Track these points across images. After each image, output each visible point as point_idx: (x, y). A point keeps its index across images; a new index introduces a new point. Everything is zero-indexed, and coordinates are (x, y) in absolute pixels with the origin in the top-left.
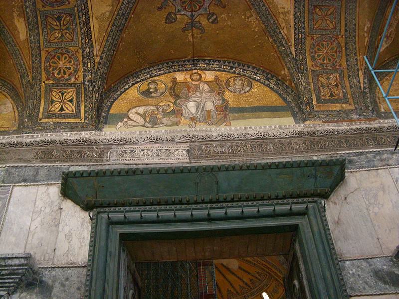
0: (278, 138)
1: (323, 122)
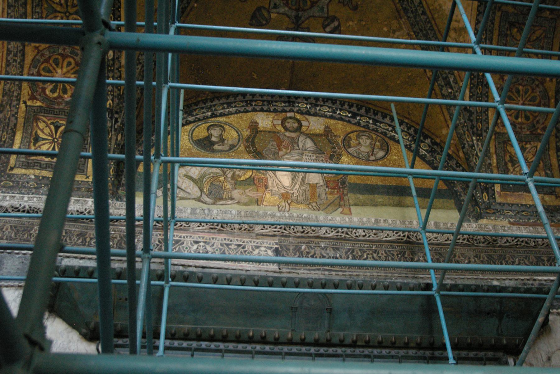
1: (510, 223)
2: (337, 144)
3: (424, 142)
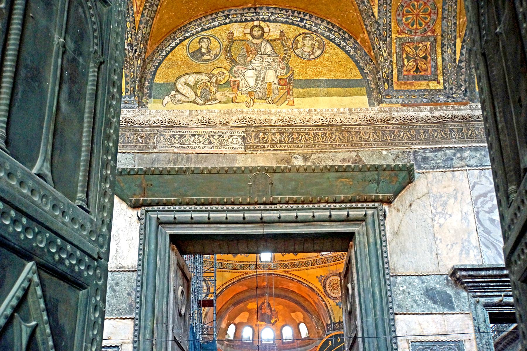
0: (345, 125)
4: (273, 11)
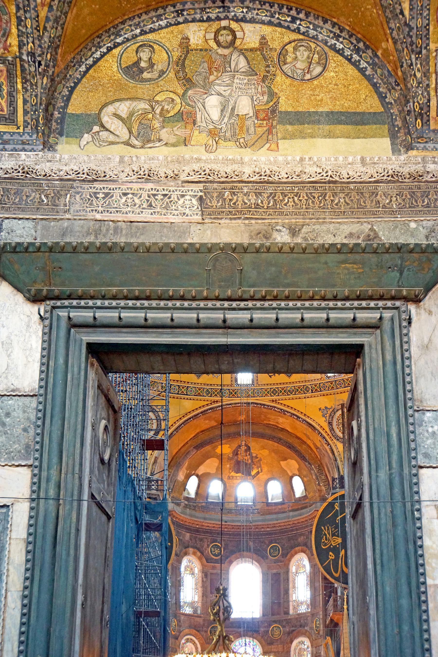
0: (355, 182)
2: (272, 61)
3: (365, 53)
4: (251, 5)
